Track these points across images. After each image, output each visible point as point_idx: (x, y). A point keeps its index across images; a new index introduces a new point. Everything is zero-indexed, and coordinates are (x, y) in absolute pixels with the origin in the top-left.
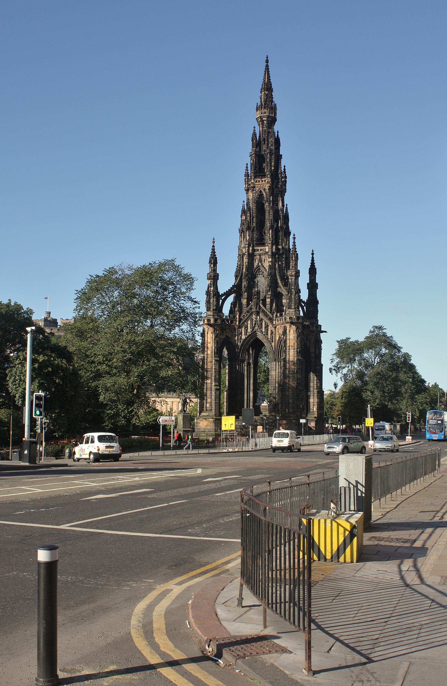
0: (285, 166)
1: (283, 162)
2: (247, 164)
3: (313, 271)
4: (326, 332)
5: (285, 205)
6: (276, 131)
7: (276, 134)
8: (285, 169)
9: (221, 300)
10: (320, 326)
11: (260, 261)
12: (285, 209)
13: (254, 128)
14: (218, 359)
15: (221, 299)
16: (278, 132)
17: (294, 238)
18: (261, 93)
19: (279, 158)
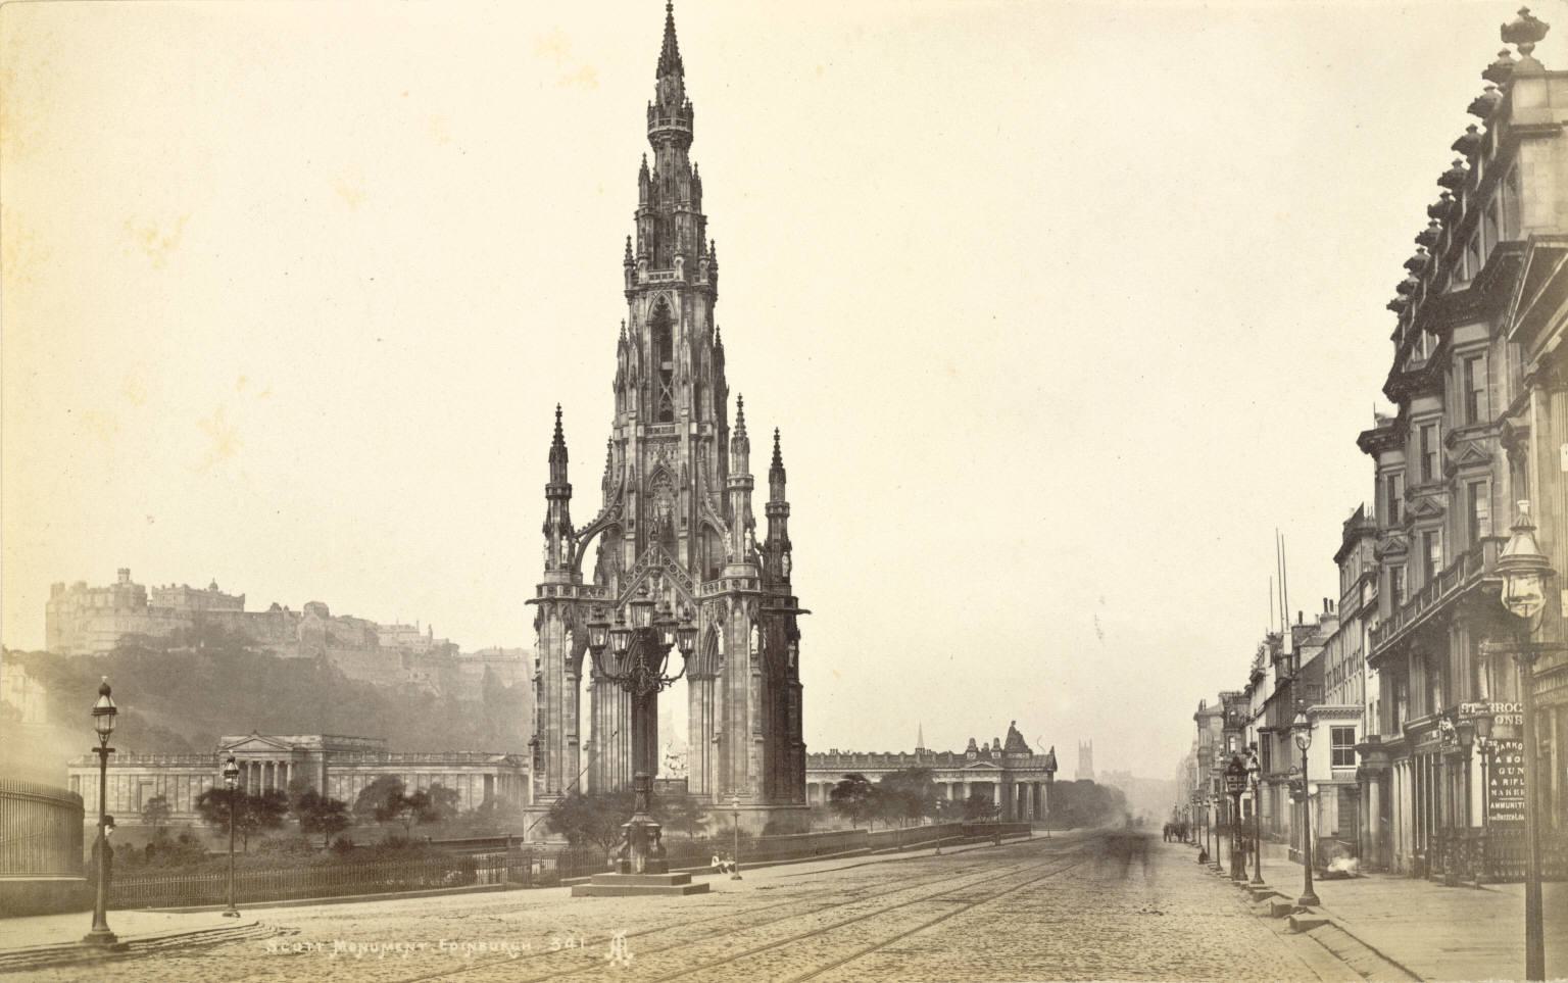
0: (713, 242)
1: (709, 235)
2: (629, 238)
3: (778, 473)
4: (808, 612)
5: (715, 327)
6: (692, 162)
7: (693, 168)
8: (713, 249)
9: (577, 545)
10: (796, 599)
11: (662, 455)
12: (715, 337)
13: (645, 155)
14: (571, 675)
15: (578, 541)
16: (696, 165)
17: (740, 404)
18: (658, 78)
19: (701, 222)
